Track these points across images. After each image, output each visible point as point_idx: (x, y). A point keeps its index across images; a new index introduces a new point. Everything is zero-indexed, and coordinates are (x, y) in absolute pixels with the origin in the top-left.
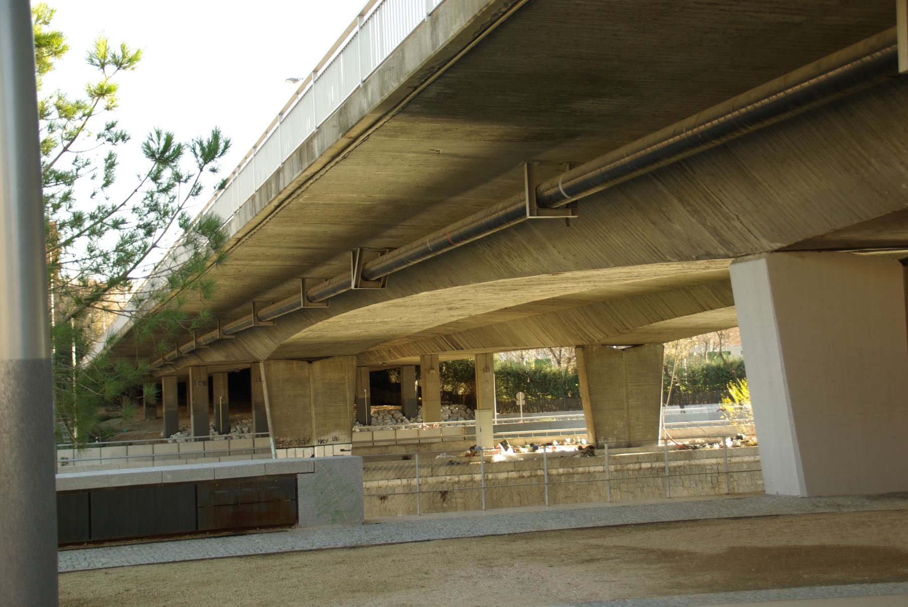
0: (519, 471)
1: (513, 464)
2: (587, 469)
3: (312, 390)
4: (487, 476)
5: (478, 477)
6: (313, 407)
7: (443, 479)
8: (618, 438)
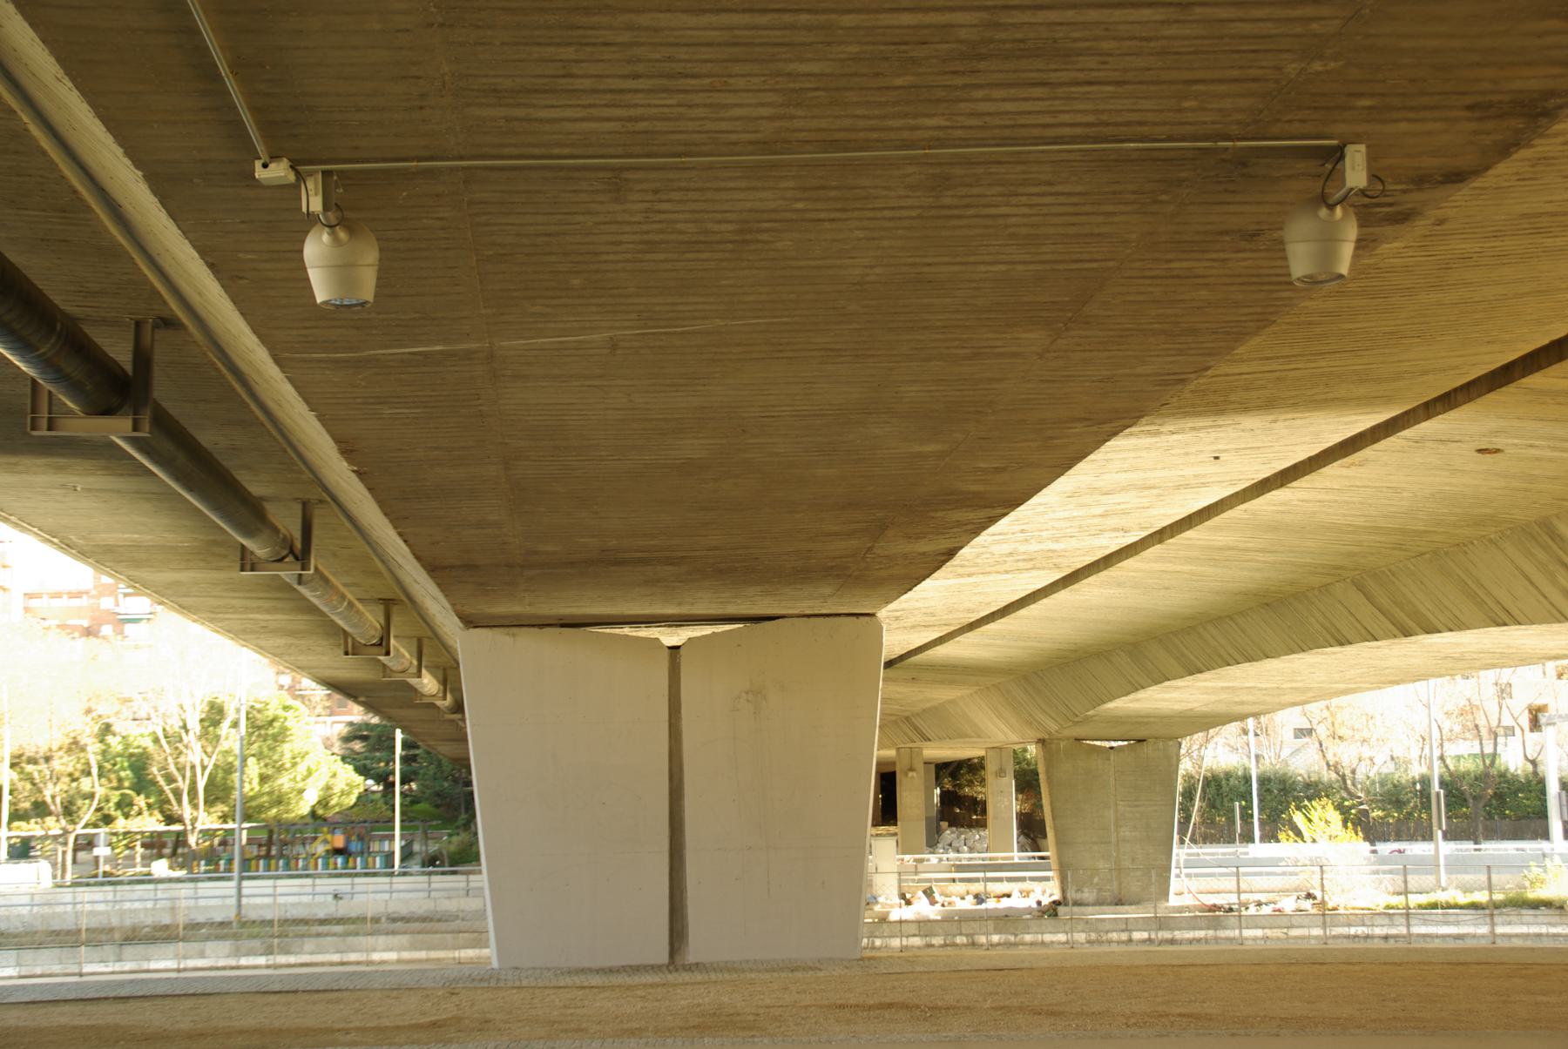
0: (926, 936)
2: (1040, 936)
4: (873, 942)
8: (1100, 890)
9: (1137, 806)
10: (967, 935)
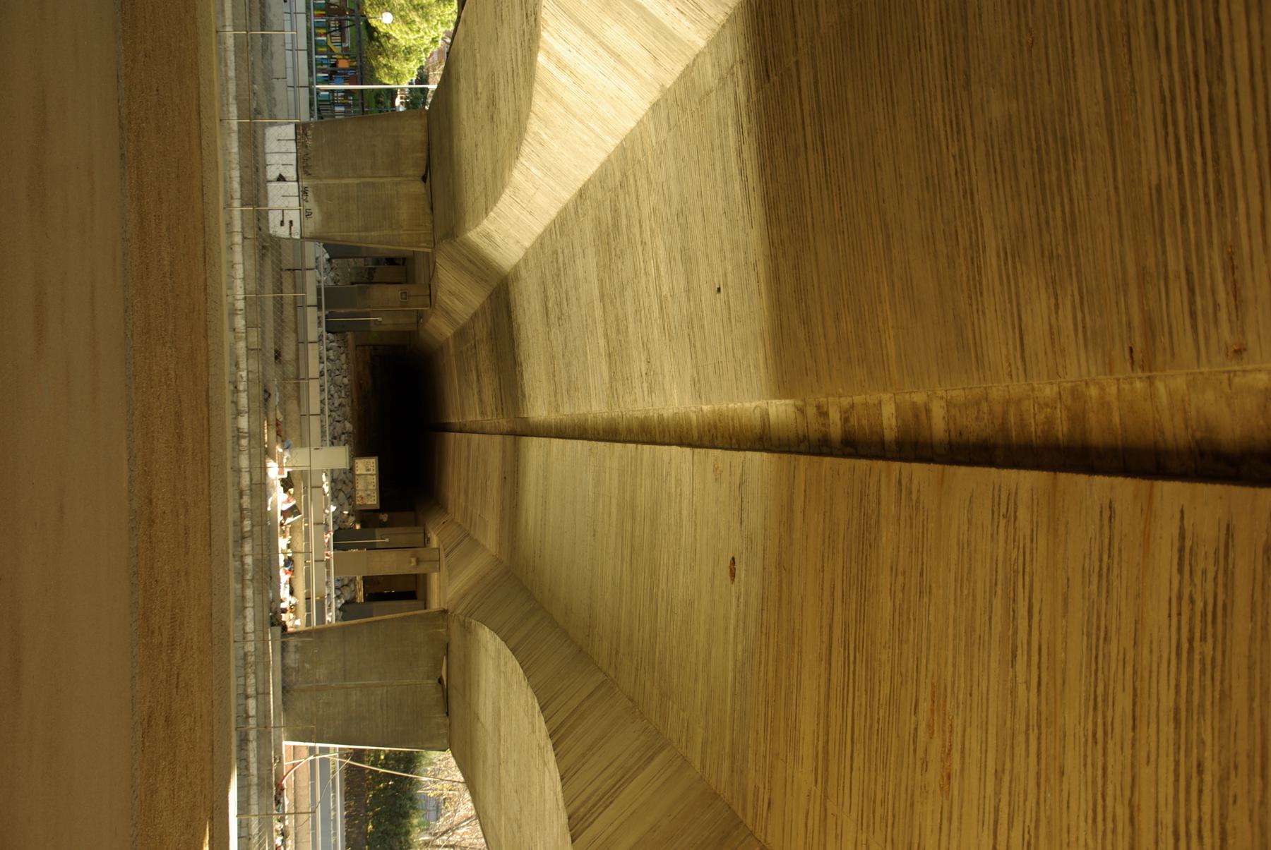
0: (251, 490)
1: (261, 489)
3: (382, 180)
4: (245, 437)
5: (243, 423)
7: (243, 365)
9: (382, 709)
10: (251, 531)
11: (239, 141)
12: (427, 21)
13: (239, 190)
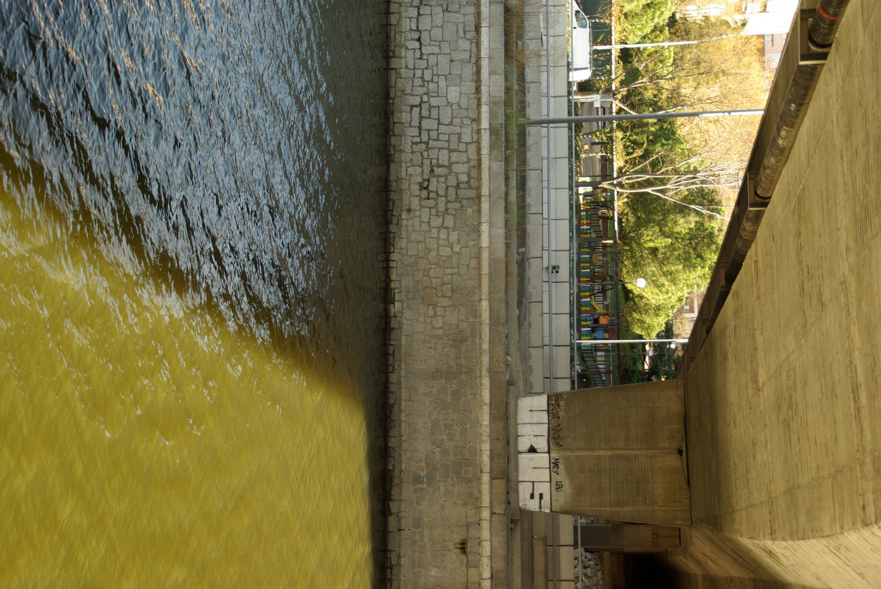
3: (637, 452)
6: (609, 453)
11: (491, 413)
12: (675, 284)
13: (488, 464)
